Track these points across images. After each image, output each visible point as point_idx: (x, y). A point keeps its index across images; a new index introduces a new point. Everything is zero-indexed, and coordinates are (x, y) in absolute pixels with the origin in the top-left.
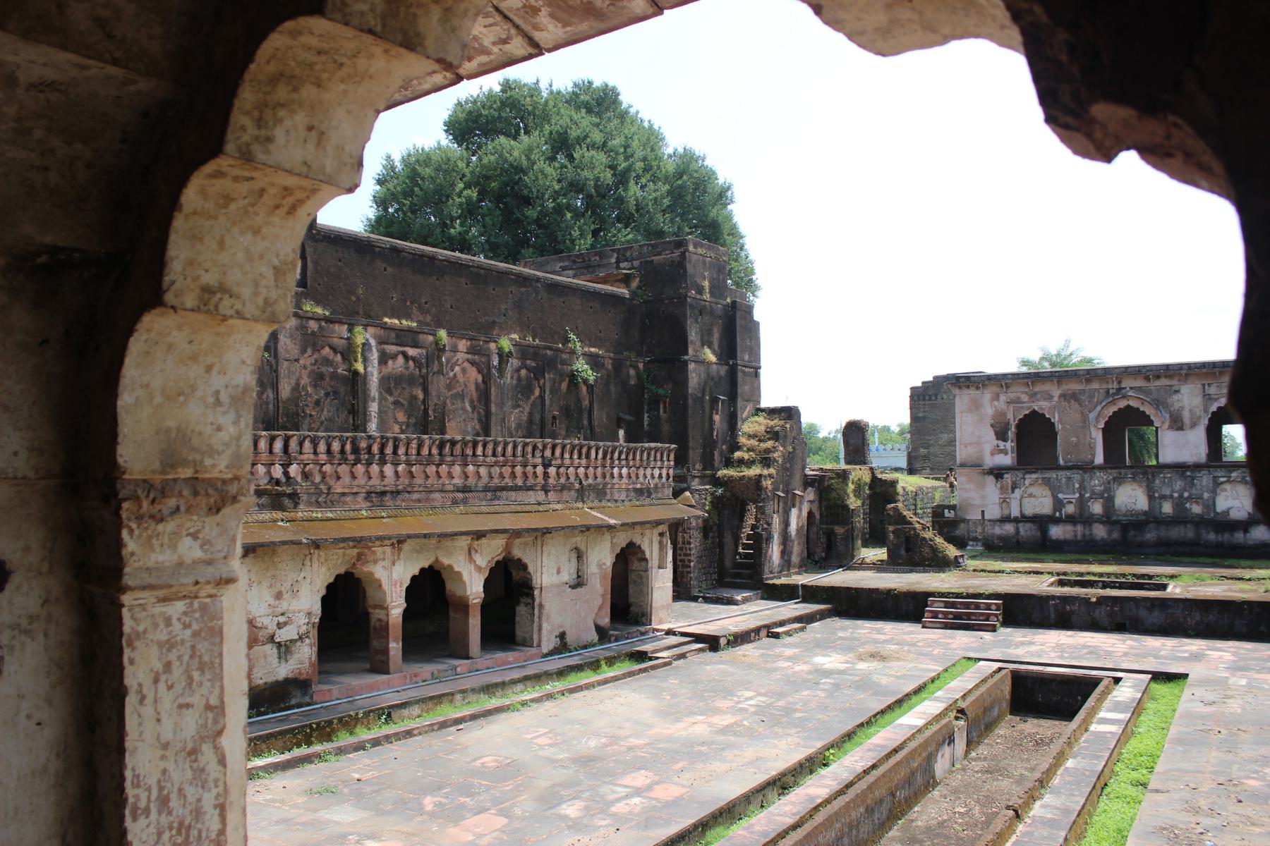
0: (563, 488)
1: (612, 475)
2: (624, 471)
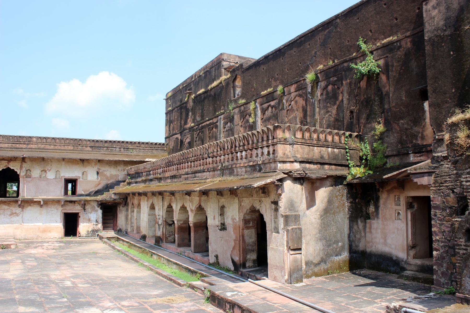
0: (214, 170)
1: (237, 156)
2: (244, 153)
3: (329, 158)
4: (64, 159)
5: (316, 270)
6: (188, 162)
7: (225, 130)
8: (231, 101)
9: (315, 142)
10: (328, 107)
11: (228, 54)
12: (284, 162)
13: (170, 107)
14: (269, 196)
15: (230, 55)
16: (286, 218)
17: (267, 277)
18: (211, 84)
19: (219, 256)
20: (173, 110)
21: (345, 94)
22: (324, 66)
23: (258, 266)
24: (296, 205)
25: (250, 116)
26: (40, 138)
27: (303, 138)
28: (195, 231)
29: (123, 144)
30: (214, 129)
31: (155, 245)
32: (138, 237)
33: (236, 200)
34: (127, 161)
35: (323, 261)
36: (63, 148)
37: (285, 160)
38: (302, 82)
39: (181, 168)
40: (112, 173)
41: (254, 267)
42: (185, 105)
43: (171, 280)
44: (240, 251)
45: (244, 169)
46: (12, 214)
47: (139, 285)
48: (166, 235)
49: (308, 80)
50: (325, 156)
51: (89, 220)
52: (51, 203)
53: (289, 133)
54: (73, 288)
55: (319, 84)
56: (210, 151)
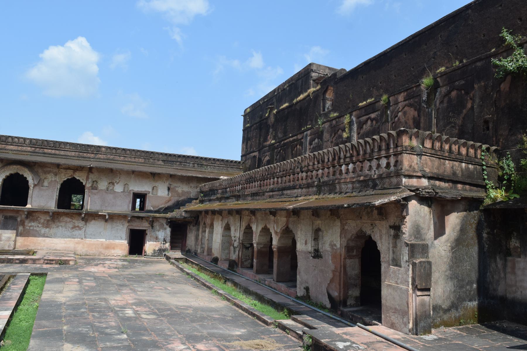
0: (308, 186)
1: (341, 170)
3: (462, 175)
4: (133, 172)
5: (446, 317)
6: (274, 178)
7: (312, 147)
8: (320, 115)
9: (447, 154)
10: (450, 117)
11: (318, 65)
12: (410, 177)
13: (248, 123)
14: (386, 219)
15: (320, 65)
16: (412, 248)
17: (381, 323)
18: (297, 97)
19: (310, 289)
20: (251, 127)
21: (477, 101)
22: (447, 68)
23: (361, 305)
24: (423, 232)
25: (344, 130)
26: (110, 148)
27: (433, 148)
28: (279, 257)
29: (197, 160)
30: (298, 146)
31: (228, 269)
32: (208, 259)
33: (338, 223)
34: (200, 177)
35: (454, 306)
36: (133, 160)
37: (412, 174)
38: (414, 89)
39: (265, 184)
40: (184, 189)
41: (356, 306)
42: (265, 121)
43: (254, 315)
44: (340, 285)
45: (350, 186)
46: (74, 227)
47: (215, 319)
48: (242, 259)
49: (423, 87)
50: (458, 172)
51: (157, 239)
52: (116, 218)
53: (417, 141)
54: (136, 318)
55: (439, 90)
56: (303, 165)
